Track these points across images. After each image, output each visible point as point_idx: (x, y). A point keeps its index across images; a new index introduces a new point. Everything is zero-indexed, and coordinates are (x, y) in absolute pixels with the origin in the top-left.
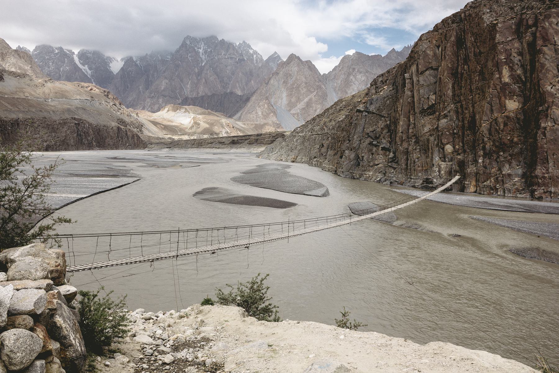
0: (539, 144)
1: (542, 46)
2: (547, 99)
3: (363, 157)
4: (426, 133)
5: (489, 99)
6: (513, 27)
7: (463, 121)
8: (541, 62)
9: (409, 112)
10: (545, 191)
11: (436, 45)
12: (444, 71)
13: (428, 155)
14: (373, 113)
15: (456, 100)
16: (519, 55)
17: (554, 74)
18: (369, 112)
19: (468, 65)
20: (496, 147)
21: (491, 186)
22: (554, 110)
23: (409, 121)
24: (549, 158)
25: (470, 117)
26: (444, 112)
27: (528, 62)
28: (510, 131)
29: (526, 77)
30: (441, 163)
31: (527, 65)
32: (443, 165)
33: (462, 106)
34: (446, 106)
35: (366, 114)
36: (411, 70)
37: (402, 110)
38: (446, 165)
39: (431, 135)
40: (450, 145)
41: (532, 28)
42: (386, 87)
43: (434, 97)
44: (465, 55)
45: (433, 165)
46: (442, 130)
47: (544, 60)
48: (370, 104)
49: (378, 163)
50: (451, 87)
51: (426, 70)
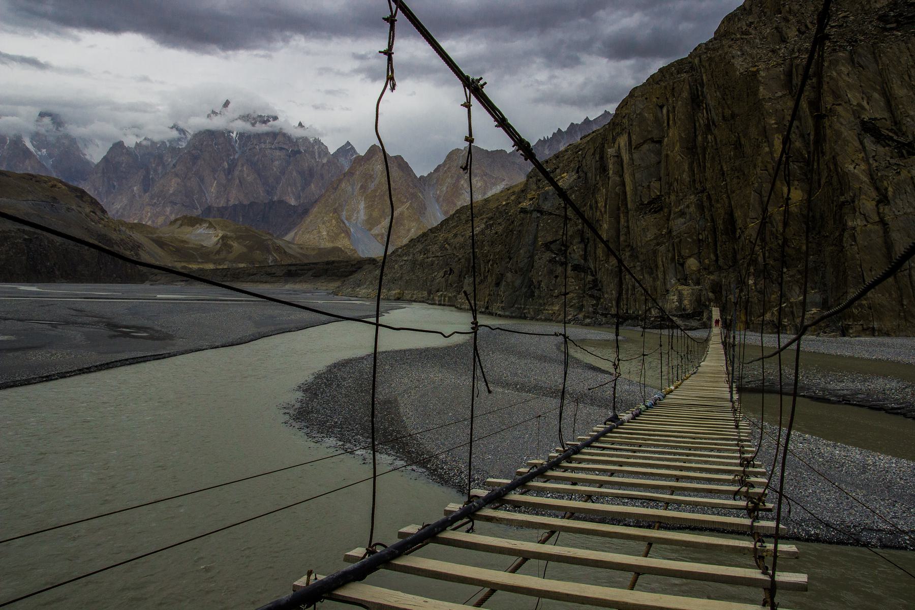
0: (848, 253)
1: (833, 104)
2: (851, 184)
3: (539, 282)
4: (651, 240)
5: (756, 185)
6: (782, 77)
7: (713, 220)
8: (836, 128)
9: (619, 209)
10: (865, 327)
11: (657, 105)
12: (673, 143)
13: (657, 275)
14: (550, 214)
17: (856, 147)
18: (541, 212)
19: (712, 134)
20: (775, 260)
21: (773, 321)
22: (864, 201)
23: (619, 222)
24: (865, 275)
25: (725, 213)
26: (680, 208)
28: (794, 234)
29: (809, 153)
30: (680, 288)
31: (809, 134)
32: (686, 290)
33: (709, 197)
34: (681, 198)
35: (539, 215)
36: (617, 143)
37: (605, 206)
38: (690, 291)
39: (658, 244)
40: (695, 258)
41: (812, 79)
42: (565, 174)
43: (655, 185)
44: (708, 119)
45: (667, 291)
46: (679, 235)
47: (839, 125)
48: (544, 200)
50: (687, 169)
51: (644, 142)
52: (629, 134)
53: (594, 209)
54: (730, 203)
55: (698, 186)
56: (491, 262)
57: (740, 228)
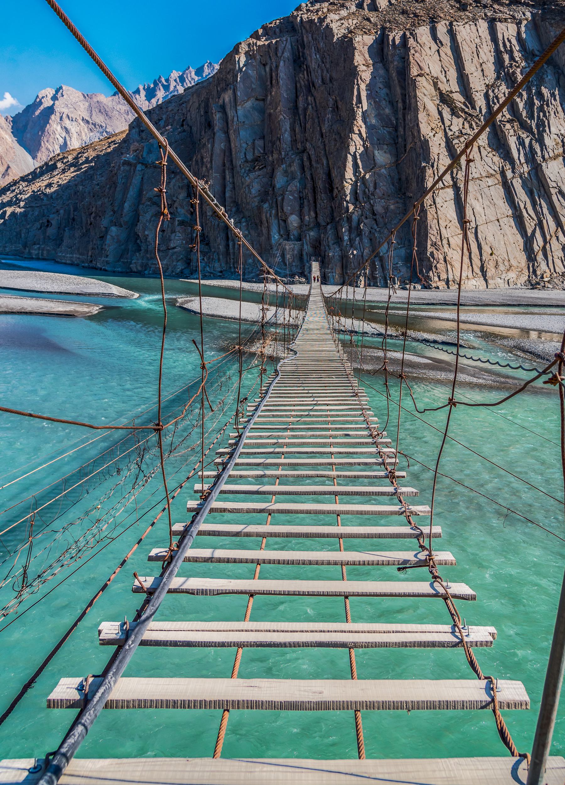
13: (262, 231)
15: (298, 149)
16: (386, 87)
19: (312, 95)
27: (399, 98)
31: (397, 101)
33: (309, 158)
35: (143, 167)
42: (170, 127)
44: (308, 80)
49: (175, 245)
52: (234, 89)
53: (200, 165)
54: (328, 164)
55: (299, 146)
56: (93, 215)
57: (337, 188)
